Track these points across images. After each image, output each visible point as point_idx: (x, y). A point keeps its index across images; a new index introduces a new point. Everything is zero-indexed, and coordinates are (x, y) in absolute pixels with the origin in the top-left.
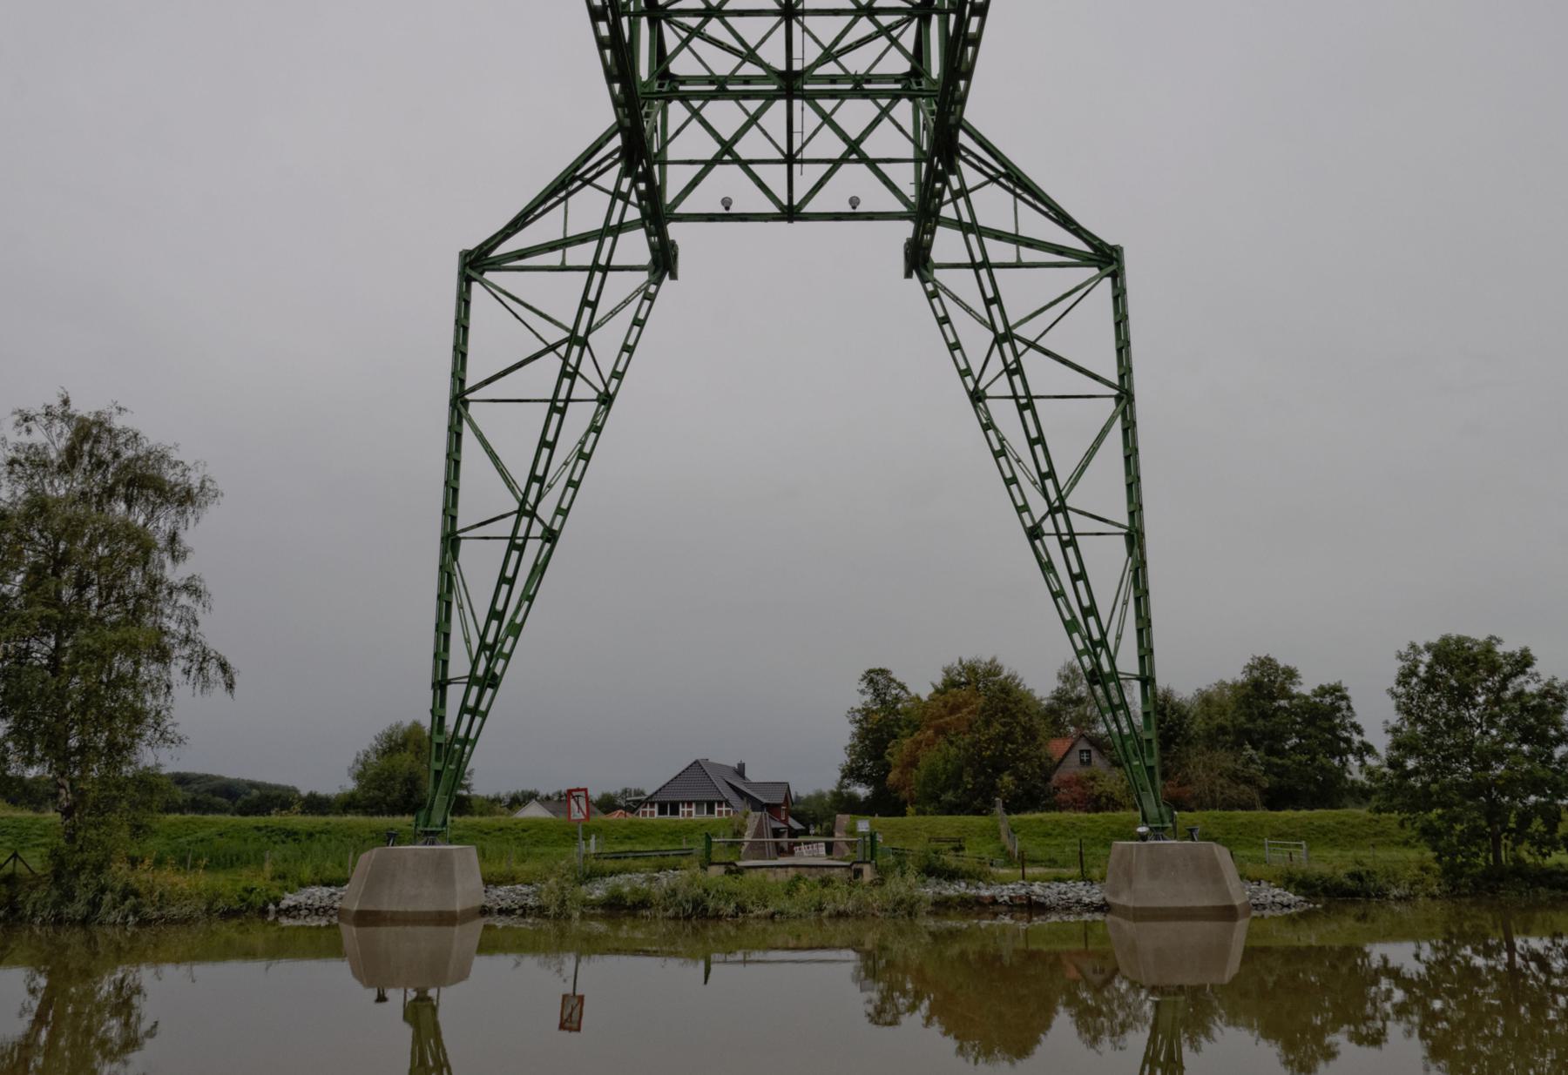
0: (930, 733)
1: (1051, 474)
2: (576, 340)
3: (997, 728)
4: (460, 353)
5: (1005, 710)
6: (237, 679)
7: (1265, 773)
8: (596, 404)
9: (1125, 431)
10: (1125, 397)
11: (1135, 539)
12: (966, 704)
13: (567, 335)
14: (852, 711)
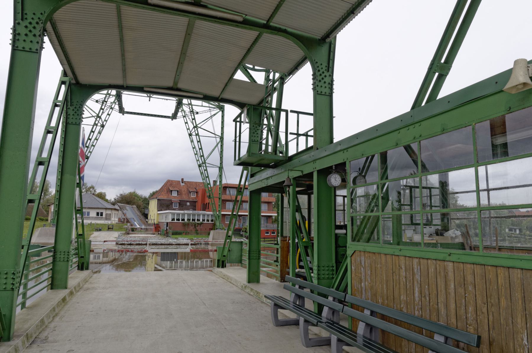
1: (203, 156)
2: (98, 117)
8: (100, 127)
9: (221, 146)
10: (222, 138)
13: (96, 115)
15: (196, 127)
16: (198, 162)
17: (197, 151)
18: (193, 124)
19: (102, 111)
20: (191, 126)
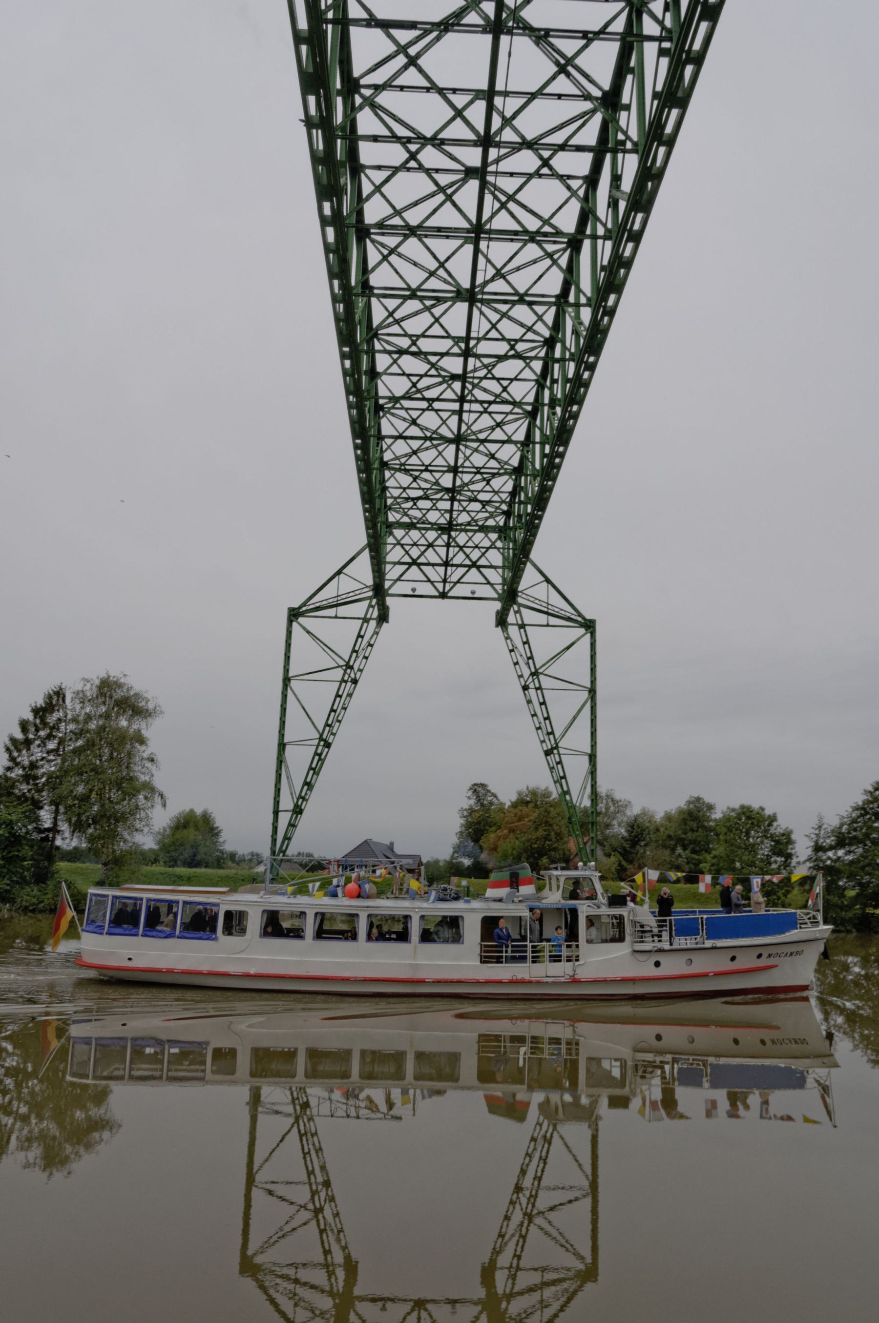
0: (506, 831)
1: (552, 733)
2: (349, 666)
3: (541, 833)
4: (287, 658)
5: (546, 822)
6: (167, 802)
7: (688, 863)
10: (592, 692)
11: (592, 757)
12: (528, 816)
14: (462, 810)
15: (535, 674)
16: (544, 744)
17: (540, 723)
18: (529, 668)
19: (354, 655)
20: (526, 673)
